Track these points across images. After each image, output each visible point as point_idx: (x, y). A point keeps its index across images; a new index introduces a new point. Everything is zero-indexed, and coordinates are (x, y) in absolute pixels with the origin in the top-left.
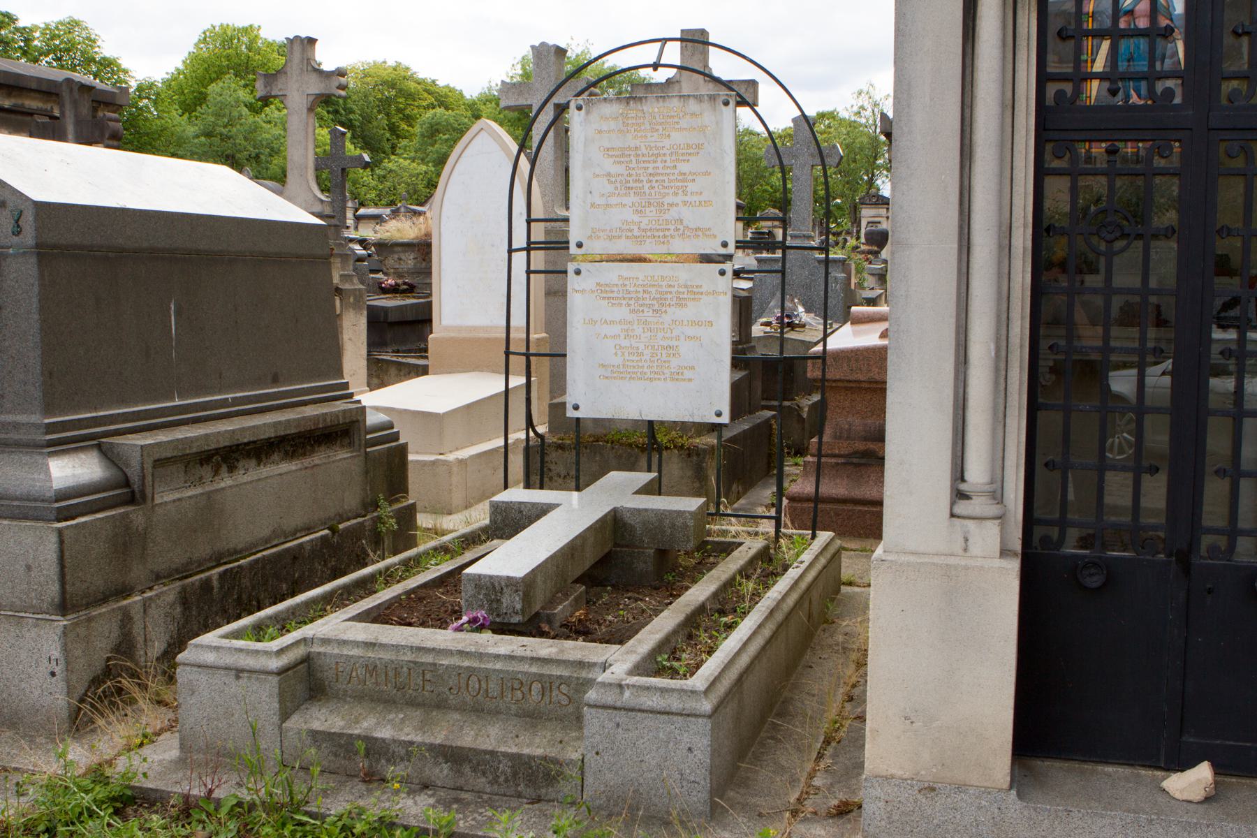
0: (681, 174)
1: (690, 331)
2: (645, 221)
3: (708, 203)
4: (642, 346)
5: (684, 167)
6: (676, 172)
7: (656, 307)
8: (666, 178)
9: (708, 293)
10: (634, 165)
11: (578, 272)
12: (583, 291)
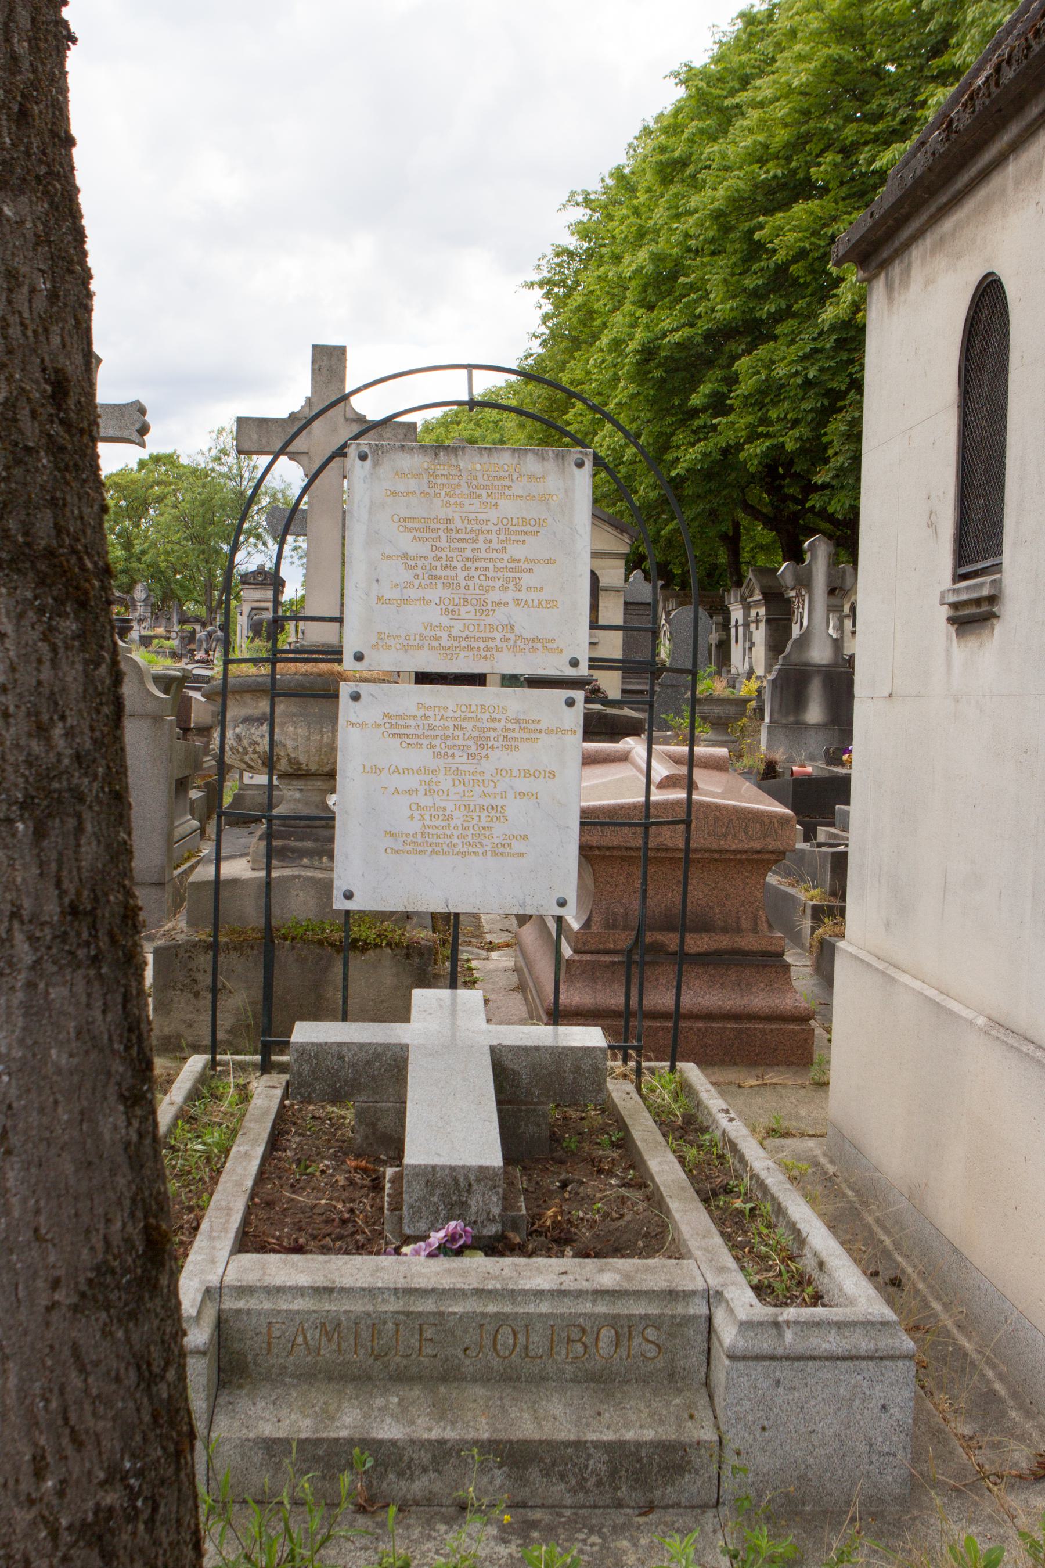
0: (513, 560)
3: (551, 603)
4: (450, 807)
5: (516, 551)
6: (506, 557)
7: (473, 750)
8: (491, 566)
9: (549, 732)
10: (443, 544)
11: (356, 697)
12: (362, 725)
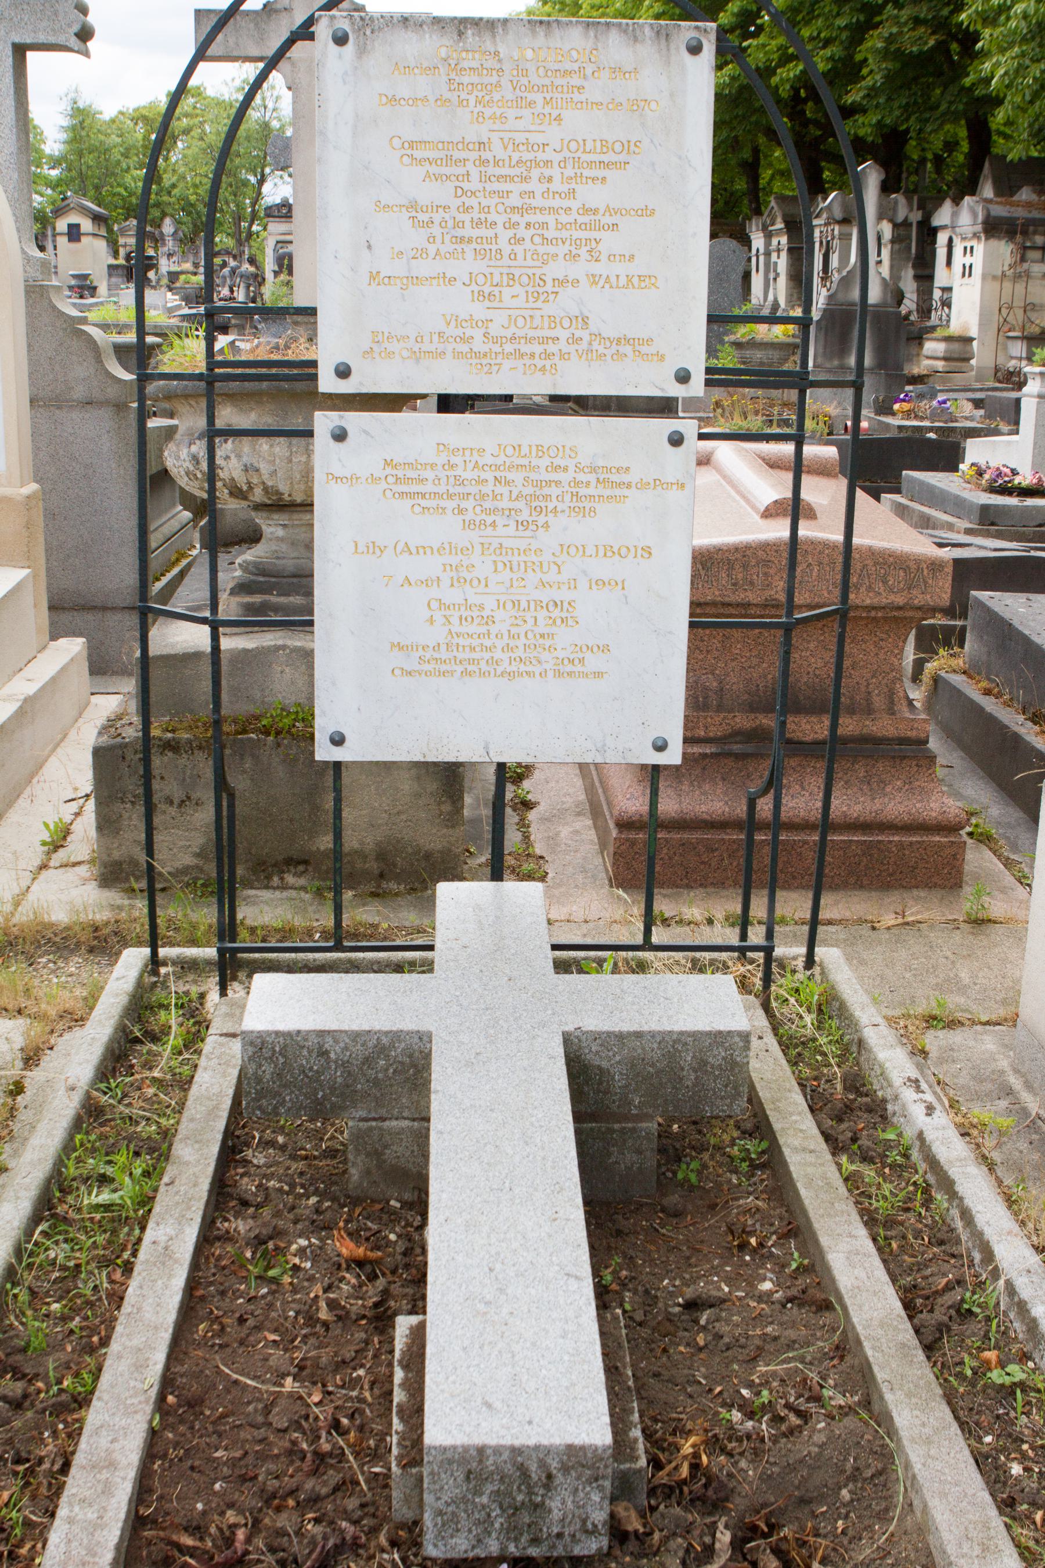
0: (586, 210)
1: (603, 568)
2: (500, 318)
3: (647, 280)
4: (490, 603)
5: (592, 195)
6: (575, 205)
7: (525, 515)
8: (550, 219)
9: (642, 485)
10: (474, 184)
11: (340, 436)
12: (353, 479)
